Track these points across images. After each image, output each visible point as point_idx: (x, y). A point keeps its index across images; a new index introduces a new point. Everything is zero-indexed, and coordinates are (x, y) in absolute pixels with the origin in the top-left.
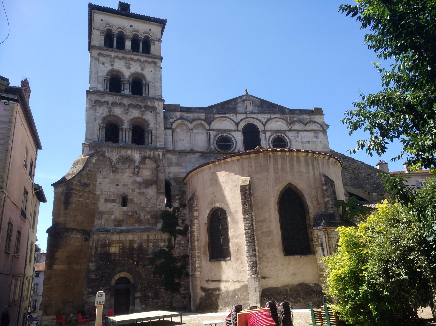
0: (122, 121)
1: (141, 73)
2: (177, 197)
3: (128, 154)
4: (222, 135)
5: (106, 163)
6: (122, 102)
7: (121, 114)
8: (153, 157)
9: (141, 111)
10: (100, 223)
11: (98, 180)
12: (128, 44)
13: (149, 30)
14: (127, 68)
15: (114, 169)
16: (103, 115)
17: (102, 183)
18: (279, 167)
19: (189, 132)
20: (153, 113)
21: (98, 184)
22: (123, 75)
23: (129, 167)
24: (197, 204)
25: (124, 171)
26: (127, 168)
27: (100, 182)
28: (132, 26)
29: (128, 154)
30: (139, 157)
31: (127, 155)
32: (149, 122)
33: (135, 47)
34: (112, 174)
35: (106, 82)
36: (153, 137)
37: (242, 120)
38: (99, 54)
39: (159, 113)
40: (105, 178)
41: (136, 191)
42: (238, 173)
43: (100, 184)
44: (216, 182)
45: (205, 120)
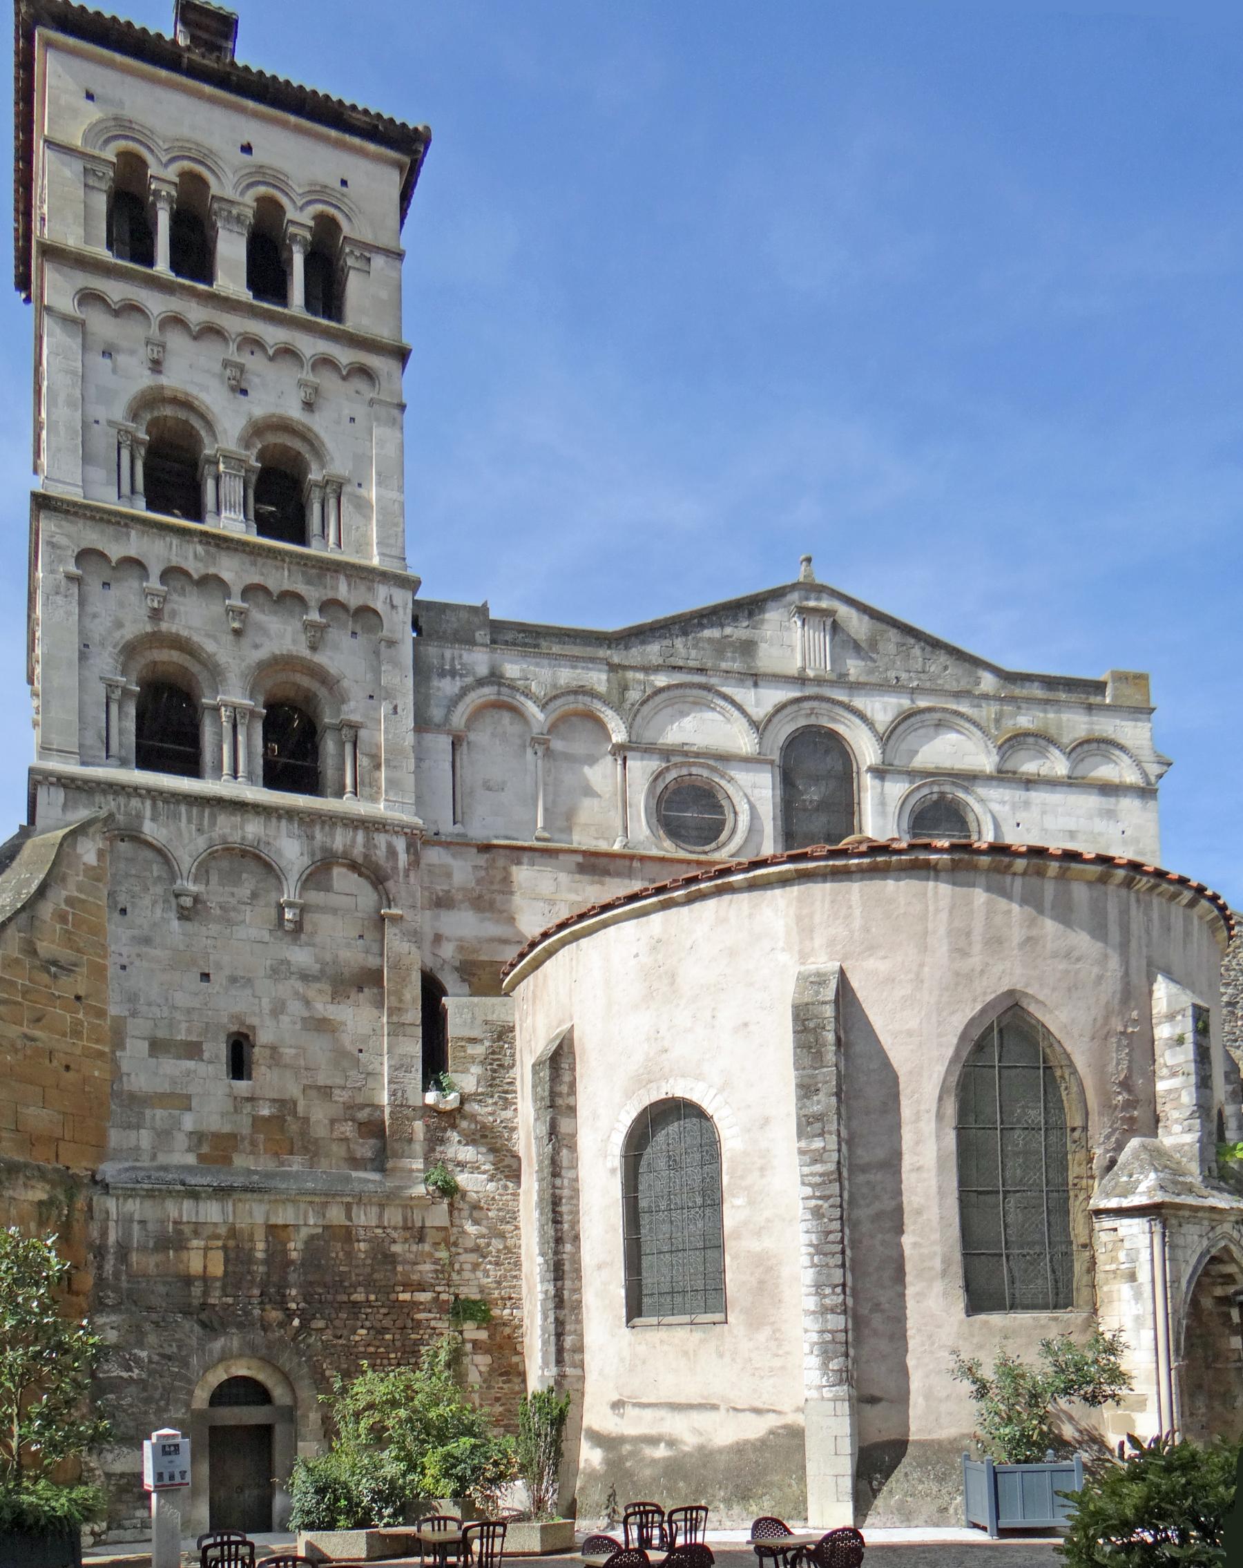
0: (216, 673)
1: (304, 425)
2: (478, 1050)
4: (684, 771)
5: (148, 874)
7: (208, 635)
9: (308, 626)
10: (133, 1143)
11: (113, 948)
14: (233, 389)
15: (187, 902)
17: (132, 963)
19: (529, 751)
20: (362, 639)
21: (112, 971)
22: (209, 425)
23: (254, 895)
25: (232, 914)
26: (244, 903)
27: (124, 961)
28: (247, 149)
29: (250, 836)
30: (302, 854)
31: (243, 838)
32: (345, 683)
34: (175, 923)
35: (125, 454)
38: (88, 297)
39: (391, 643)
40: (147, 941)
42: (781, 944)
43: (124, 967)
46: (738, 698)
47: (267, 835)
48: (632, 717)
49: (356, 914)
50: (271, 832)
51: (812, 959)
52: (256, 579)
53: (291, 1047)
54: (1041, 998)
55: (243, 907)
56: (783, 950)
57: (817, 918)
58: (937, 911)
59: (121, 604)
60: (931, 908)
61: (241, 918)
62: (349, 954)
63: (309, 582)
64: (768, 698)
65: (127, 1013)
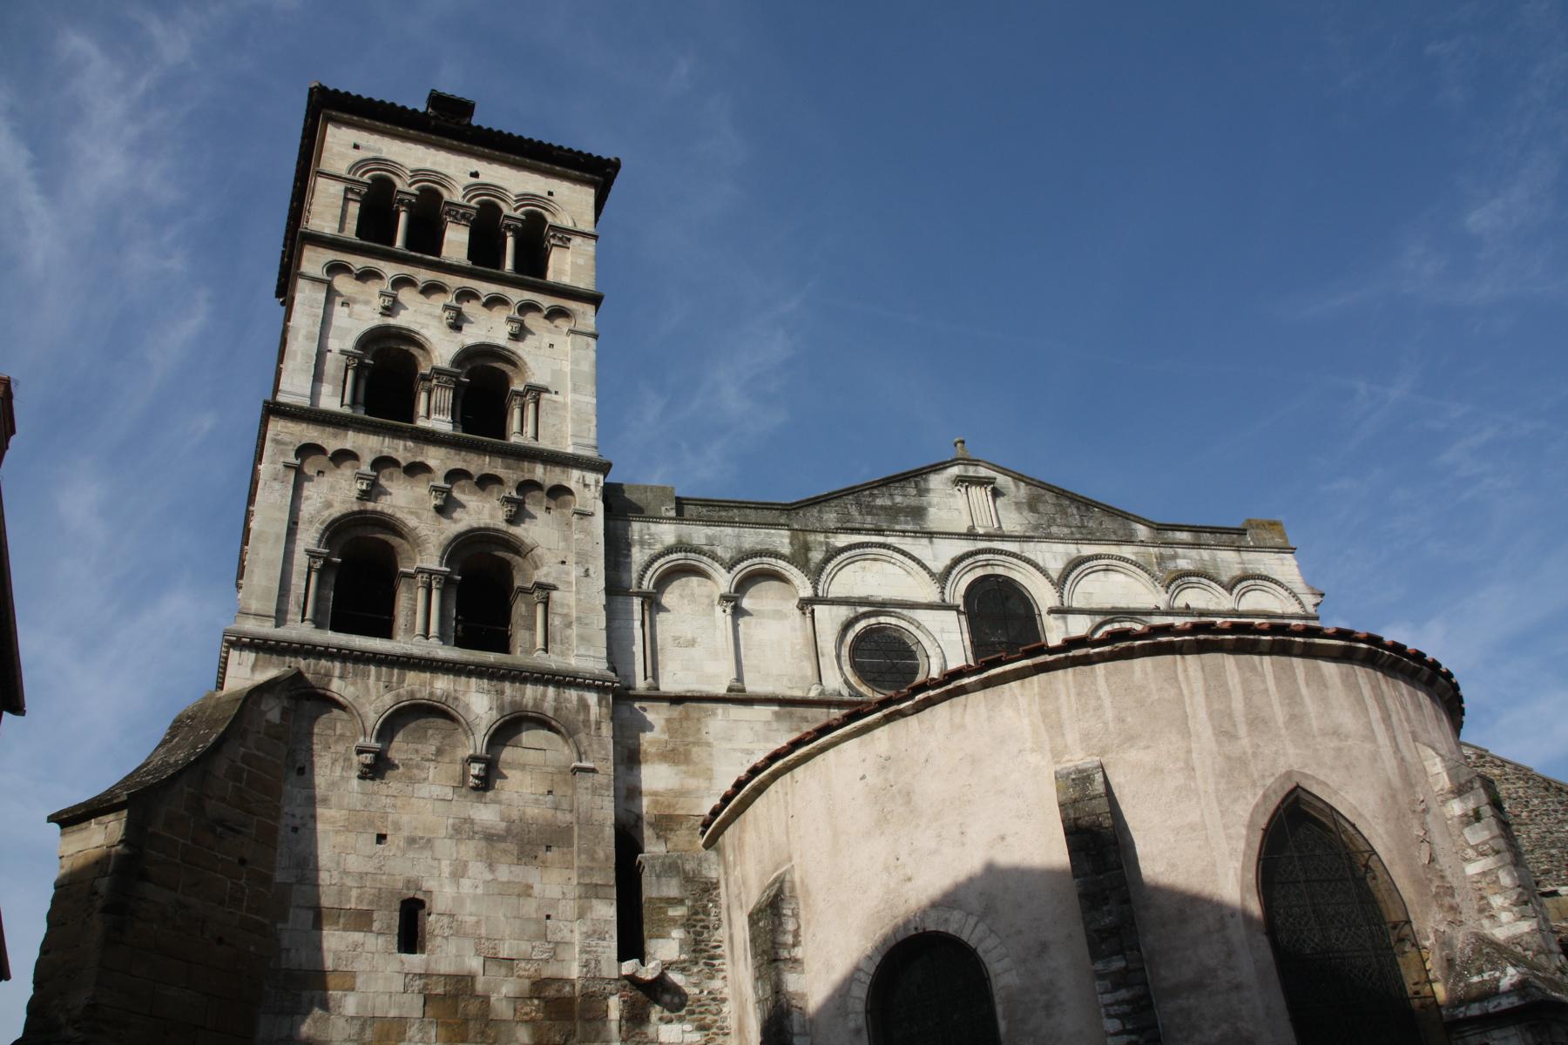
0: (417, 543)
3: (439, 692)
5: (330, 732)
6: (419, 459)
8: (556, 710)
11: (286, 809)
12: (456, 242)
13: (546, 195)
16: (331, 511)
18: (1238, 704)
19: (719, 609)
24: (796, 934)
25: (415, 771)
27: (297, 822)
29: (439, 692)
30: (491, 709)
31: (431, 694)
33: (484, 252)
36: (556, 621)
37: (957, 561)
41: (470, 873)
42: (1029, 745)
43: (295, 830)
44: (908, 802)
45: (790, 560)
46: (915, 554)
47: (455, 691)
48: (815, 574)
49: (545, 769)
50: (461, 688)
51: (1067, 757)
52: (459, 465)
53: (471, 915)
54: (1322, 778)
55: (427, 764)
56: (1032, 750)
57: (1065, 713)
58: (1192, 693)
59: (332, 488)
60: (1185, 692)
61: (424, 775)
62: (536, 811)
63: (508, 467)
64: (941, 553)
65: (293, 880)
